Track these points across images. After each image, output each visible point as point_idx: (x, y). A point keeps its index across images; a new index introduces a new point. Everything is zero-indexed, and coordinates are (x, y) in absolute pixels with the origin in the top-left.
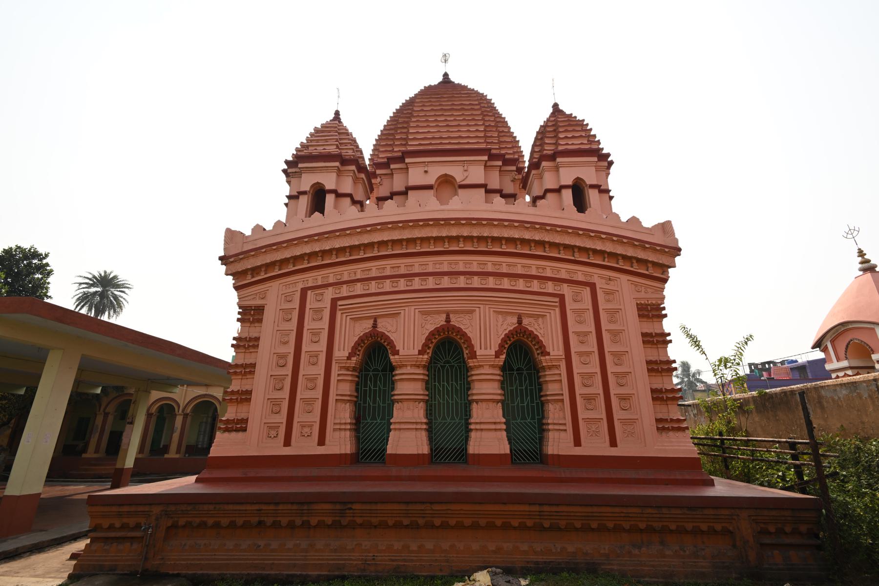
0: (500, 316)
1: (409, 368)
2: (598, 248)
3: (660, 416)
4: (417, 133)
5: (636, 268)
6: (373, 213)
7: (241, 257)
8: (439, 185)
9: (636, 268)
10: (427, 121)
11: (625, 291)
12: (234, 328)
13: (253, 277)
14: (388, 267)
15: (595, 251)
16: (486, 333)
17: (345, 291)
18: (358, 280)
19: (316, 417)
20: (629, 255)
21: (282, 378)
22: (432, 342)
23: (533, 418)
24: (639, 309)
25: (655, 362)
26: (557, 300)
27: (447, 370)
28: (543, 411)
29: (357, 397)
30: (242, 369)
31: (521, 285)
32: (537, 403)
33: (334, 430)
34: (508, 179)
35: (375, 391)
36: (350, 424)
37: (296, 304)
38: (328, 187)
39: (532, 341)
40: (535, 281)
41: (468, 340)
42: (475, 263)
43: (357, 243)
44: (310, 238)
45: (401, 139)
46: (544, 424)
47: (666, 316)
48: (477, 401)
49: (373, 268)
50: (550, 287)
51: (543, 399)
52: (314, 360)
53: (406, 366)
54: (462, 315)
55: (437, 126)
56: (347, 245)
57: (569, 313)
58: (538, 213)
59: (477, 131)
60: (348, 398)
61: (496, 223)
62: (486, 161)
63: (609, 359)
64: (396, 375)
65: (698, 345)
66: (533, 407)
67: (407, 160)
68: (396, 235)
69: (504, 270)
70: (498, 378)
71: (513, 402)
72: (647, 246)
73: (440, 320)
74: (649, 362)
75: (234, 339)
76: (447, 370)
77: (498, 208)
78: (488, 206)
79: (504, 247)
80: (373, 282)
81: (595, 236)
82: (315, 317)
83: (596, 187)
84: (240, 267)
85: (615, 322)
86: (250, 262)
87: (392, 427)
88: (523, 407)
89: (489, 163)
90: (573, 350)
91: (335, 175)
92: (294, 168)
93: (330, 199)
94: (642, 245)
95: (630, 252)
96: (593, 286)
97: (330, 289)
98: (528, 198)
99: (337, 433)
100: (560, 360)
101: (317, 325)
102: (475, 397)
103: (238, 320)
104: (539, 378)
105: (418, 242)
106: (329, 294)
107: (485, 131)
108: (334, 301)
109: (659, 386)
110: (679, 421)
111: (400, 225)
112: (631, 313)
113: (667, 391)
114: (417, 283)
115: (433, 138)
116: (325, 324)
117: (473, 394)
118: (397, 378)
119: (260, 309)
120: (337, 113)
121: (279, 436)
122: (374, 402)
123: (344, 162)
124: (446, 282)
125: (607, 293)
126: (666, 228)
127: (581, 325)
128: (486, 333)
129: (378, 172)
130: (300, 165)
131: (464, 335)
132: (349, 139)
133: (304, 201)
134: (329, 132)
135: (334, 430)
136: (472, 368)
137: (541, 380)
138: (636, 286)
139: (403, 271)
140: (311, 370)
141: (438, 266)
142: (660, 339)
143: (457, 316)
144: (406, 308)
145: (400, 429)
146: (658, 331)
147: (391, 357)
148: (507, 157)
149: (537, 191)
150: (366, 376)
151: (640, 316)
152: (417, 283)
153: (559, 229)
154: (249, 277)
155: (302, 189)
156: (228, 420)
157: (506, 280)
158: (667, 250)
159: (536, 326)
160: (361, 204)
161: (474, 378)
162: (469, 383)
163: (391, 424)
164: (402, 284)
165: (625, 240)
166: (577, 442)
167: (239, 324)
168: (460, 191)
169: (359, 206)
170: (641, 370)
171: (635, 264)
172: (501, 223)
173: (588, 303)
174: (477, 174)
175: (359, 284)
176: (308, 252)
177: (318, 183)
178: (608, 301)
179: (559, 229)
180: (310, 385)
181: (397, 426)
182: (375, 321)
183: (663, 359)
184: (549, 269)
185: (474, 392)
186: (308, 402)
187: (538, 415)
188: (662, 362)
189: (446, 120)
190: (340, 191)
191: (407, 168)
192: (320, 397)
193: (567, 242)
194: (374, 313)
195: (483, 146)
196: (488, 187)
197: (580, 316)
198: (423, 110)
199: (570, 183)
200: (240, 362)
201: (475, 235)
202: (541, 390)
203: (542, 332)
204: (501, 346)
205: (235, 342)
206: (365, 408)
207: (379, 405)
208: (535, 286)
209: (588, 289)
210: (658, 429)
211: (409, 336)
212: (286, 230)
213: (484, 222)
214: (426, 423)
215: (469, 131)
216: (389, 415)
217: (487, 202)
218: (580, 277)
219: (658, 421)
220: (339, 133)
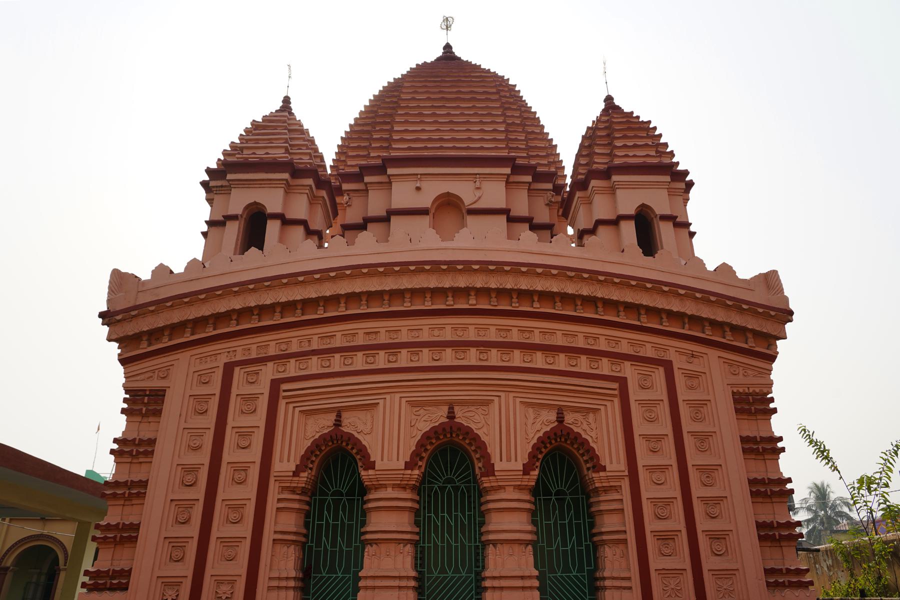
0: (531, 410)
1: (390, 490)
2: (675, 310)
4: (406, 131)
5: (729, 339)
6: (337, 251)
7: (133, 313)
8: (438, 208)
9: (729, 339)
10: (420, 115)
11: (714, 376)
12: (118, 425)
13: (150, 345)
14: (361, 332)
15: (671, 314)
16: (508, 434)
17: (292, 368)
18: (314, 352)
19: (240, 567)
20: (720, 319)
21: (188, 505)
22: (426, 450)
23: (581, 570)
24: (736, 401)
25: (762, 482)
26: (615, 385)
27: (449, 493)
28: (596, 559)
29: (306, 536)
30: (126, 490)
31: (561, 362)
32: (587, 546)
33: (270, 588)
34: (540, 202)
35: (335, 527)
36: (295, 578)
37: (216, 388)
38: (271, 209)
39: (578, 449)
40: (584, 358)
41: (482, 446)
42: (493, 329)
43: (314, 295)
44: (243, 287)
45: (381, 139)
46: (597, 579)
47: (774, 411)
48: (495, 543)
49: (339, 335)
50: (605, 367)
51: (595, 539)
52: (240, 476)
53: (385, 486)
54: (472, 408)
55: (436, 122)
56: (299, 298)
58: (586, 256)
59: (495, 131)
60: (293, 538)
61: (524, 269)
62: (508, 175)
64: (369, 501)
65: (826, 457)
66: (580, 552)
67: (390, 171)
68: (373, 285)
69: (537, 339)
70: (528, 506)
71: (550, 544)
72: (745, 307)
73: (439, 416)
74: (752, 482)
75: (116, 441)
76: (449, 493)
77: (527, 247)
78: (512, 245)
79: (536, 305)
80: (337, 356)
81: (670, 292)
82: (245, 408)
83: (671, 218)
84: (131, 329)
85: (701, 420)
86: (147, 323)
87: (361, 584)
88: (565, 552)
89: (512, 179)
90: (640, 463)
91: (281, 192)
92: (217, 181)
93: (273, 228)
94: (738, 305)
95: (720, 316)
96: (668, 366)
97: (270, 365)
98: (570, 231)
99: (274, 594)
100: (621, 478)
101: (247, 420)
102: (491, 537)
103: (123, 411)
104: (590, 506)
105: (408, 296)
106: (269, 372)
107: (506, 131)
108: (275, 385)
110: (799, 572)
111: (381, 269)
112: (724, 407)
114: (404, 359)
115: (430, 140)
116: (260, 419)
117: (489, 532)
118: (370, 505)
119: (158, 395)
120: (287, 100)
122: (334, 545)
123: (297, 172)
124: (448, 357)
125: (692, 376)
126: (770, 280)
127: (651, 425)
128: (508, 434)
129: (345, 187)
130: (229, 177)
131: (476, 438)
132: (304, 139)
133: (233, 231)
134: (275, 128)
135: (270, 588)
136: (487, 491)
137: (593, 509)
138: (731, 365)
139: (383, 339)
140: (239, 492)
141: (436, 332)
143: (466, 409)
144: (388, 397)
145: (374, 588)
146: (764, 434)
147: (363, 473)
148: (539, 169)
149: (584, 222)
150: (322, 502)
151: (737, 411)
152: (404, 359)
153: (617, 280)
154: (144, 344)
155: (231, 212)
157: (539, 354)
158: (773, 313)
159: (585, 426)
160: (319, 235)
161: (491, 506)
162: (482, 514)
163: (360, 579)
164: (381, 360)
165: (713, 298)
167: (124, 417)
168: (470, 219)
169: (316, 238)
170: (740, 493)
171: (729, 334)
172: (532, 270)
173: (660, 391)
174: (494, 194)
175: (315, 358)
176: (238, 307)
177: (255, 203)
178: (691, 388)
179: (617, 280)
180: (233, 516)
181: (370, 583)
182: (339, 416)
184: (603, 339)
185: (491, 527)
186: (230, 542)
187: (589, 565)
188: (771, 481)
189: (448, 115)
190: (290, 215)
191: (390, 183)
192: (248, 534)
193: (630, 300)
194: (337, 402)
195: (504, 153)
196: (512, 214)
198: (413, 99)
199: (631, 211)
200: (122, 479)
201: (493, 286)
202: (592, 525)
203: (593, 434)
204: (532, 456)
205: (115, 446)
206: (318, 553)
207: (341, 550)
208: (583, 364)
209: (661, 369)
211: (390, 438)
212: (205, 275)
213: (507, 268)
214: (415, 578)
215: (482, 131)
216: (356, 566)
217: (509, 237)
218: (649, 353)
220: (290, 131)
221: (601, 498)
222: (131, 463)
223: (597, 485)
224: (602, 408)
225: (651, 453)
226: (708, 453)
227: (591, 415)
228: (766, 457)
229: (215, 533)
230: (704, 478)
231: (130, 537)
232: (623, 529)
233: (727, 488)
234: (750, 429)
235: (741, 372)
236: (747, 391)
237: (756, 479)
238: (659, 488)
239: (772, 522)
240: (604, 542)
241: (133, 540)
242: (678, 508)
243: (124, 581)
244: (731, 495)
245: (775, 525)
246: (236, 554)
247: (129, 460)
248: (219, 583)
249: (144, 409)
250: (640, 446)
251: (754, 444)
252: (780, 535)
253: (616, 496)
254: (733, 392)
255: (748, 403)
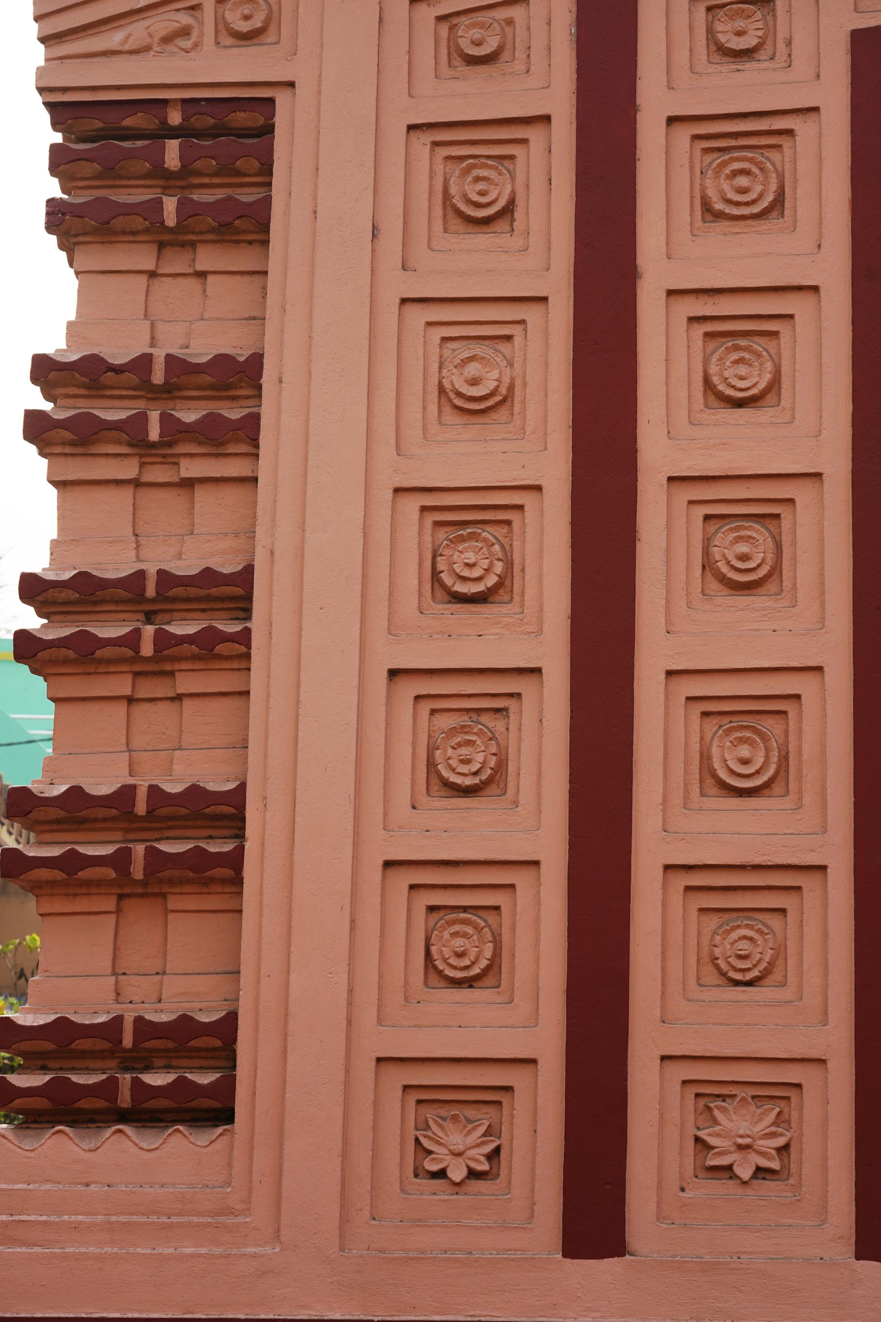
82: (720, 189)
119: (234, 133)
121: (516, 1162)
156: (62, 1031)
200: (114, 566)
222: (137, 483)
229: (652, 846)
231: (199, 860)
241: (220, 876)
243: (205, 1079)
246: (780, 950)
247: (129, 470)
248: (708, 1097)
249: (170, 205)
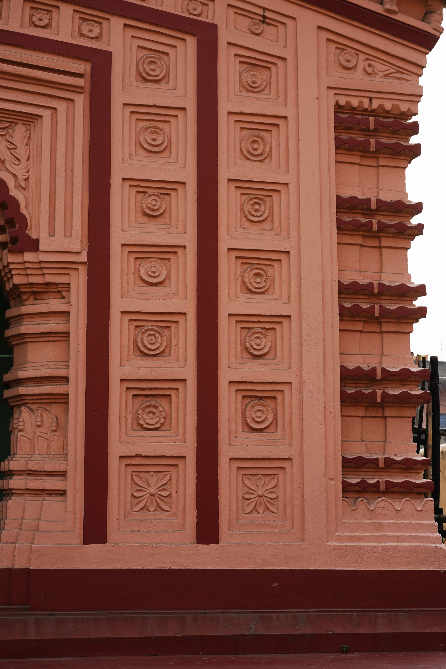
3: (358, 451)
24: (340, 125)
25: (366, 291)
51: (7, 393)
57: (119, 118)
63: (227, 271)
74: (346, 290)
96: (206, 36)
100: (72, 266)
109: (364, 363)
112: (311, 135)
113: (389, 377)
125: (257, 63)
138: (342, 48)
142: (391, 221)
146: (388, 197)
151: (340, 145)
166: (95, 529)
173: (182, 90)
178: (252, 88)
183: (391, 281)
188: (386, 291)
197: (155, 131)
203: (20, 171)
209: (191, 42)
210: (347, 489)
219: (350, 464)
221: (25, 309)
223: (17, 280)
224: (46, 114)
225: (146, 219)
226: (266, 226)
227: (20, 129)
228: (385, 242)
230: (249, 277)
232: (62, 373)
233: (294, 299)
234: (362, 184)
235: (361, 65)
236: (366, 105)
237: (355, 284)
238: (151, 293)
239: (374, 370)
240: (21, 400)
242: (186, 335)
244: (300, 313)
245: (379, 375)
250: (122, 203)
251: (365, 215)
252: (385, 395)
253: (56, 305)
254: (338, 108)
255: (366, 131)
